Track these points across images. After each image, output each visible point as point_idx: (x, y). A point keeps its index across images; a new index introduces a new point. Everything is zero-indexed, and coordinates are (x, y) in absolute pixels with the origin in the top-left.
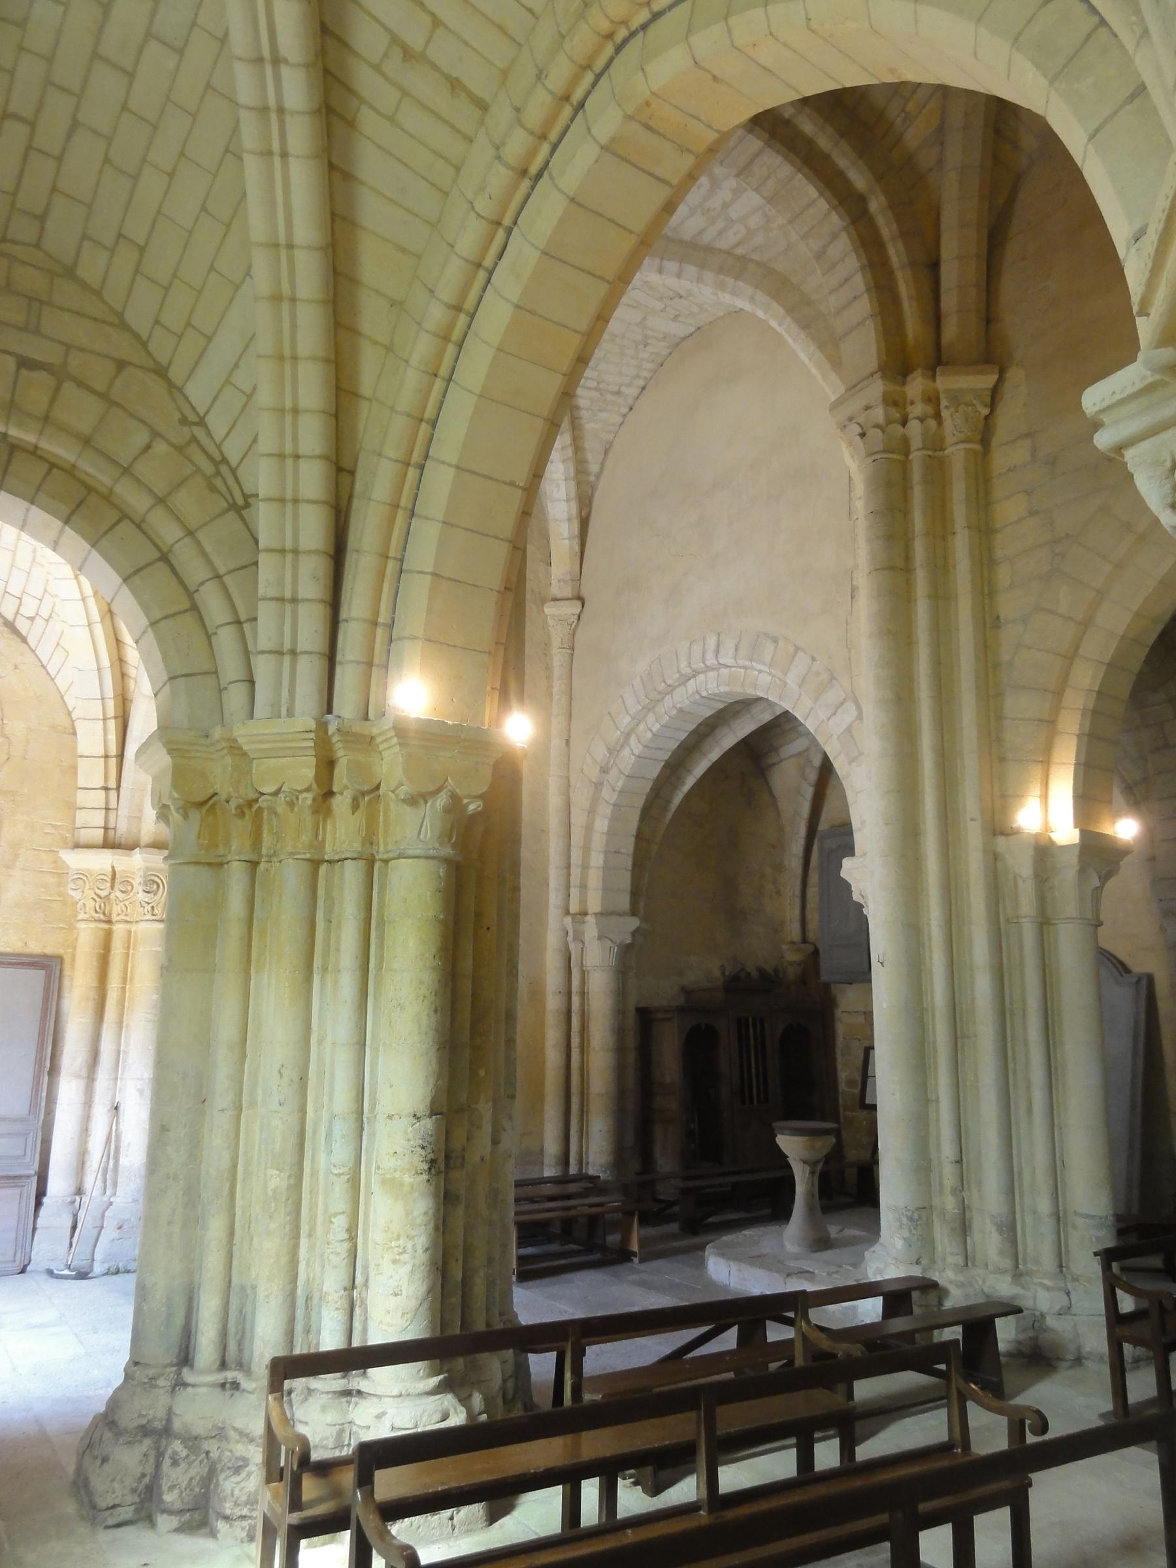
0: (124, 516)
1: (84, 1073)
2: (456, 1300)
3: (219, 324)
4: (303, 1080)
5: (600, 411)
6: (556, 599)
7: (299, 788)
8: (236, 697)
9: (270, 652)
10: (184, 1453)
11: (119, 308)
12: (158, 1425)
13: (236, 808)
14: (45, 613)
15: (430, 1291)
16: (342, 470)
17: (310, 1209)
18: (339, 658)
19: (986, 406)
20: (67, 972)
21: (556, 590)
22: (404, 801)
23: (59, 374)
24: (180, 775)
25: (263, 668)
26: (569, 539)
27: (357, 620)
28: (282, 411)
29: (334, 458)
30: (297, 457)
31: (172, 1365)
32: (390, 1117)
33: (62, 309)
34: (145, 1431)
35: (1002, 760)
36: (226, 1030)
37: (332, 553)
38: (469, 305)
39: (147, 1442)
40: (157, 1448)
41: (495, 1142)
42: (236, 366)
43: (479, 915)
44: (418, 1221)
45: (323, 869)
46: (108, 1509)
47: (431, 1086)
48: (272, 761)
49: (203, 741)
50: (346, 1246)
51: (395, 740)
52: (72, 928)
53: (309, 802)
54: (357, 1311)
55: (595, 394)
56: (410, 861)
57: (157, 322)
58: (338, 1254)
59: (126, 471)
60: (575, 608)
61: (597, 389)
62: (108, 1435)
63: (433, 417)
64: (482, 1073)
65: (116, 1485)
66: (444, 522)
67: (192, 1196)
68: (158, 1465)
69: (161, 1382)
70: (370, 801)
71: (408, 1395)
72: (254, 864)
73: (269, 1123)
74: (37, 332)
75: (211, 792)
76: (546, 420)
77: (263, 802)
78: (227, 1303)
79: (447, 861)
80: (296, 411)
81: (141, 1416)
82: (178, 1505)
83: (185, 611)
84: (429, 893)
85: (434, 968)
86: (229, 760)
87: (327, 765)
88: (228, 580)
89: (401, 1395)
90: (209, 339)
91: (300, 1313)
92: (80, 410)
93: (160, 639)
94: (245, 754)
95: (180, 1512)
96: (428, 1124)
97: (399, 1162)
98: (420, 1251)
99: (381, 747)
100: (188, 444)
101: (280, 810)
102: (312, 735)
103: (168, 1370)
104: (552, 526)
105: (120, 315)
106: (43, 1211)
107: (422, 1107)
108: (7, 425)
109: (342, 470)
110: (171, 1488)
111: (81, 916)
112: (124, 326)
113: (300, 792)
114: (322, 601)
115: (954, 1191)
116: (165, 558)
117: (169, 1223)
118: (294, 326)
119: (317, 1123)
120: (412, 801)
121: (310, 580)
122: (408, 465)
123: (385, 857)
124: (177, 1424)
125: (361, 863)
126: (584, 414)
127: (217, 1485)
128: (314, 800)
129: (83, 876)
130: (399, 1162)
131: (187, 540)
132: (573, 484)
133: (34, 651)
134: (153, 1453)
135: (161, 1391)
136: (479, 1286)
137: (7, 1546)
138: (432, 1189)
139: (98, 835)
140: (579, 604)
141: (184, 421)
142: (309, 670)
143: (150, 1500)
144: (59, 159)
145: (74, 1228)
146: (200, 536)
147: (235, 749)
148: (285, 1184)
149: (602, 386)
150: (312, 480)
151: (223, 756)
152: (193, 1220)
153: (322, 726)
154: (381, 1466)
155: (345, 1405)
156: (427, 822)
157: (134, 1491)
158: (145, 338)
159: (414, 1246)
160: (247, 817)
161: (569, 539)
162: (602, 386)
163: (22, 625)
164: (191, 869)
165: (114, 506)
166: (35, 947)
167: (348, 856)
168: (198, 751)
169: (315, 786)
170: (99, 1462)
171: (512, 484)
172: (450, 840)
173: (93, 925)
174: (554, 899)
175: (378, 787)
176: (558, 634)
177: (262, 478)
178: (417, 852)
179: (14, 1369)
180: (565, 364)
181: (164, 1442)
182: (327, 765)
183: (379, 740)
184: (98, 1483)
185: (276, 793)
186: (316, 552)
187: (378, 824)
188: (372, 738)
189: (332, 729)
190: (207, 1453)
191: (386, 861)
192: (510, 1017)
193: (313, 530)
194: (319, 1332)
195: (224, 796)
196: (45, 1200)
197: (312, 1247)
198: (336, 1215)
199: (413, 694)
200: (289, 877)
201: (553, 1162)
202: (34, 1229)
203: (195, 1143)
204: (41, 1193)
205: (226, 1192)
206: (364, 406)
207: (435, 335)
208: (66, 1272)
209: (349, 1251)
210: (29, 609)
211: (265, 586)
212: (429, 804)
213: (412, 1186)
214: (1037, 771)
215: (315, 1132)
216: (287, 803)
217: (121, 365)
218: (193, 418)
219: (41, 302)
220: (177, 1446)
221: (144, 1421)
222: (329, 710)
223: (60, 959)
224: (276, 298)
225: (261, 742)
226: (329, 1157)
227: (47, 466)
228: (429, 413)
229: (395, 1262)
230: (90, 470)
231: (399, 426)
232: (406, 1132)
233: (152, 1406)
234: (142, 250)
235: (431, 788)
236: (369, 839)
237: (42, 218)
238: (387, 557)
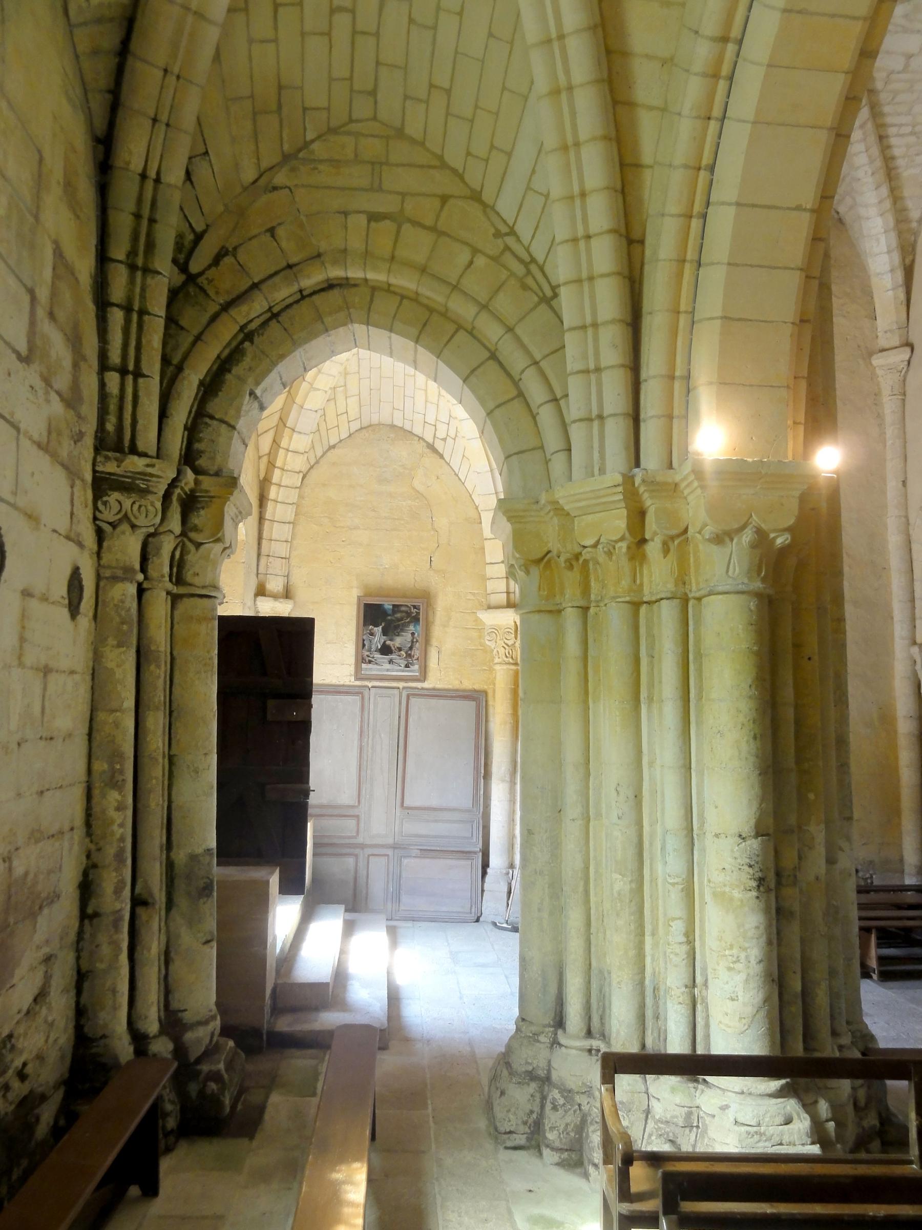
0: (459, 327)
1: (508, 779)
2: (796, 1009)
3: (515, 138)
4: (638, 798)
5: (918, 155)
6: (883, 350)
7: (614, 538)
8: (558, 465)
9: (581, 420)
10: (562, 1101)
11: (439, 152)
12: (542, 1073)
13: (565, 562)
14: (452, 433)
15: (766, 1001)
16: (631, 240)
17: (652, 911)
18: (642, 416)
20: (490, 703)
21: (883, 342)
22: (709, 540)
23: (398, 219)
24: (519, 540)
25: (577, 433)
26: (893, 289)
27: (654, 377)
28: (571, 198)
29: (623, 231)
30: (588, 237)
31: (549, 1026)
32: (717, 836)
33: (397, 165)
34: (532, 1076)
36: (572, 752)
37: (629, 321)
38: (735, 33)
40: (542, 1092)
41: (831, 861)
42: (533, 172)
43: (797, 646)
44: (750, 934)
45: (643, 609)
46: (506, 1133)
47: (754, 808)
48: (590, 517)
49: (534, 507)
50: (685, 948)
51: (696, 484)
52: (491, 670)
53: (624, 550)
54: (699, 1007)
55: (912, 139)
56: (720, 597)
57: (469, 154)
58: (677, 954)
59: (455, 287)
60: (905, 354)
61: (912, 133)
62: (505, 1073)
63: (711, 162)
64: (811, 796)
65: (511, 1116)
66: (729, 264)
67: (556, 889)
68: (542, 1107)
69: (542, 1038)
70: (679, 544)
71: (750, 1094)
72: (585, 609)
73: (612, 836)
74: (380, 189)
75: (545, 550)
76: (831, 129)
77: (586, 554)
78: (589, 982)
79: (758, 595)
80: (583, 195)
81: (527, 1063)
82: (557, 1144)
83: (513, 399)
84: (740, 626)
85: (750, 697)
86: (555, 520)
87: (638, 516)
88: (543, 364)
89: (743, 1093)
90: (509, 155)
91: (649, 1001)
92: (416, 244)
93: (495, 425)
94: (568, 514)
95: (560, 1150)
96: (754, 844)
97: (728, 878)
98: (753, 962)
99: (686, 492)
100: (502, 253)
101: (601, 560)
102: (620, 489)
103: (547, 1029)
104: (874, 281)
105: (441, 158)
106: (487, 878)
107: (747, 828)
108: (364, 270)
109: (631, 240)
110: (552, 1129)
111: (497, 660)
112: (443, 165)
113: (616, 542)
114: (623, 366)
116: (493, 356)
117: (539, 910)
118: (573, 114)
119: (653, 835)
120: (719, 539)
121: (610, 348)
122: (691, 217)
123: (697, 595)
124: (554, 1076)
125: (676, 602)
126: (900, 162)
127: (588, 1136)
128: (628, 548)
129: (495, 630)
130: (728, 878)
131: (508, 336)
132: (893, 235)
133: (448, 464)
134: (538, 1095)
135: (542, 1046)
136: (822, 998)
137: (433, 1146)
138: (762, 905)
139: (503, 598)
140: (908, 350)
141: (498, 234)
142: (615, 432)
143: (539, 1134)
144: (377, 35)
145: (509, 892)
146: (519, 331)
147: (559, 510)
148: (627, 887)
149: (917, 129)
150: (604, 255)
151: (552, 518)
152: (558, 910)
153: (628, 480)
154: (683, 1199)
155: (693, 1090)
156: (734, 559)
157: (525, 1123)
158: (461, 171)
159: (747, 957)
160: (575, 569)
161: (893, 289)
162: (917, 129)
163: (439, 445)
164: (536, 617)
165: (395, 293)
166: (468, 685)
167: (663, 596)
168: (532, 516)
169: (627, 535)
170: (499, 1093)
171: (798, 208)
172: (759, 575)
173: (505, 667)
174: (900, 630)
175: (686, 531)
176: (887, 383)
177: (561, 268)
178: (727, 588)
179: (461, 998)
180: (847, 58)
181: (546, 1088)
182: (638, 516)
183: (683, 485)
184: (499, 1112)
185: (595, 546)
186: (613, 321)
187: (689, 565)
188: (676, 485)
189: (638, 481)
190: (580, 1105)
191: (699, 599)
192: (842, 742)
193: (608, 300)
194: (666, 1019)
195: (555, 553)
196: (489, 870)
197: (656, 945)
198: (673, 919)
199: (714, 437)
200: (614, 619)
201: (914, 871)
202: (483, 891)
203: (555, 845)
204: (485, 865)
205: (581, 889)
206: (647, 175)
207: (705, 75)
208: (505, 925)
209: (688, 953)
210: (441, 434)
211: (572, 364)
212: (735, 541)
213: (742, 901)
215: (651, 844)
216: (605, 552)
217: (444, 199)
218: (504, 229)
219: (381, 164)
220: (555, 1094)
221: (530, 1068)
222: (637, 464)
224: (555, 92)
225: (580, 501)
226: (666, 866)
227: (399, 298)
228: (706, 160)
229: (730, 969)
230: (429, 293)
231: (678, 179)
232: (732, 851)
233: (534, 1056)
234: (448, 92)
235: (736, 526)
236: (682, 580)
237: (373, 93)
238: (679, 312)
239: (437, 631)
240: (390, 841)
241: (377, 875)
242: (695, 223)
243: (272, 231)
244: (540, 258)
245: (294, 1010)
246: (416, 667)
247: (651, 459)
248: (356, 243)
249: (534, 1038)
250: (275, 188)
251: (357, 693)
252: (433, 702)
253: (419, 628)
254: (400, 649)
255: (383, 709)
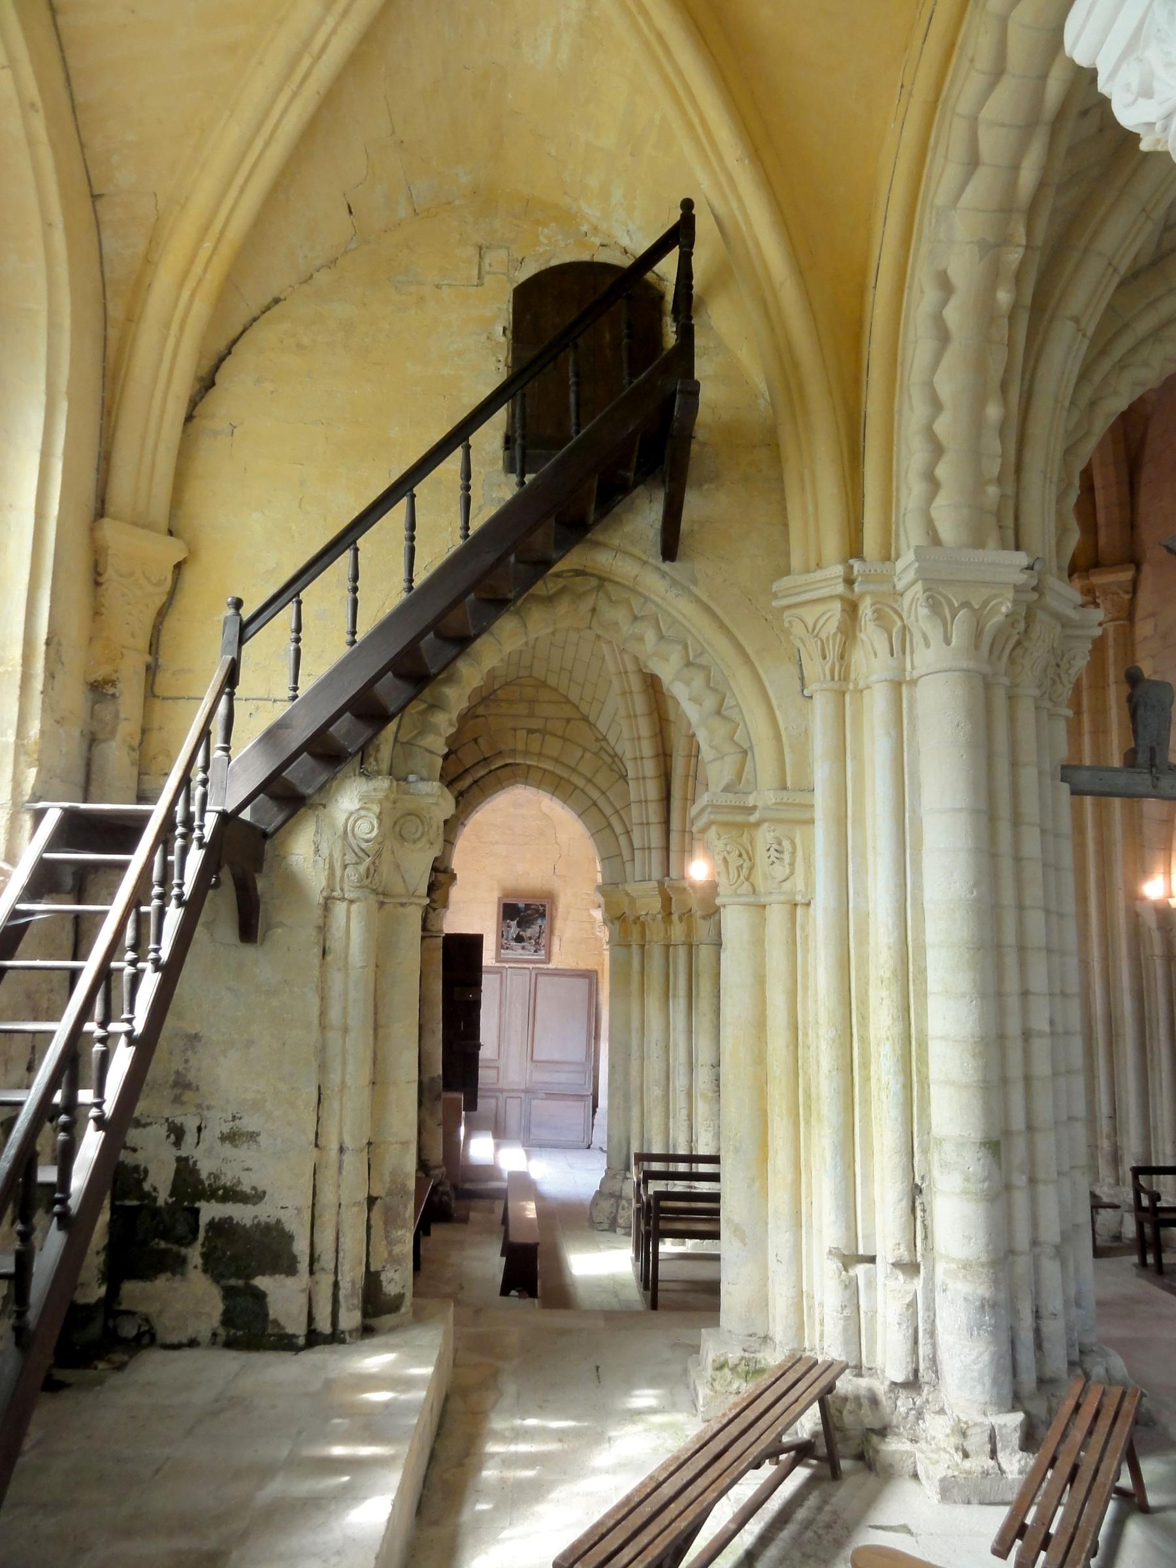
8: (628, 866)
19: (1127, 593)
34: (612, 1195)
35: (1143, 846)
36: (635, 1023)
39: (613, 1200)
67: (627, 1098)
73: (654, 1068)
80: (639, 738)
87: (667, 901)
92: (553, 746)
93: (595, 841)
105: (566, 697)
112: (568, 701)
115: (1108, 1137)
116: (595, 804)
120: (704, 918)
121: (654, 813)
141: (597, 740)
142: (656, 857)
147: (628, 894)
152: (627, 1109)
153: (661, 883)
166: (582, 966)
193: (652, 790)
197: (675, 1123)
200: (656, 952)
203: (627, 1074)
204: (595, 1106)
214: (1160, 856)
217: (568, 720)
220: (624, 1202)
223: (596, 972)
226: (679, 1082)
234: (571, 672)
237: (531, 667)
239: (559, 924)
240: (523, 1087)
241: (513, 1112)
242: (693, 760)
243: (475, 740)
244: (620, 754)
245: (472, 1181)
246: (543, 952)
247: (674, 873)
248: (520, 746)
249: (614, 1176)
250: (477, 717)
251: (497, 973)
252: (556, 979)
253: (545, 922)
254: (530, 938)
255: (518, 984)
